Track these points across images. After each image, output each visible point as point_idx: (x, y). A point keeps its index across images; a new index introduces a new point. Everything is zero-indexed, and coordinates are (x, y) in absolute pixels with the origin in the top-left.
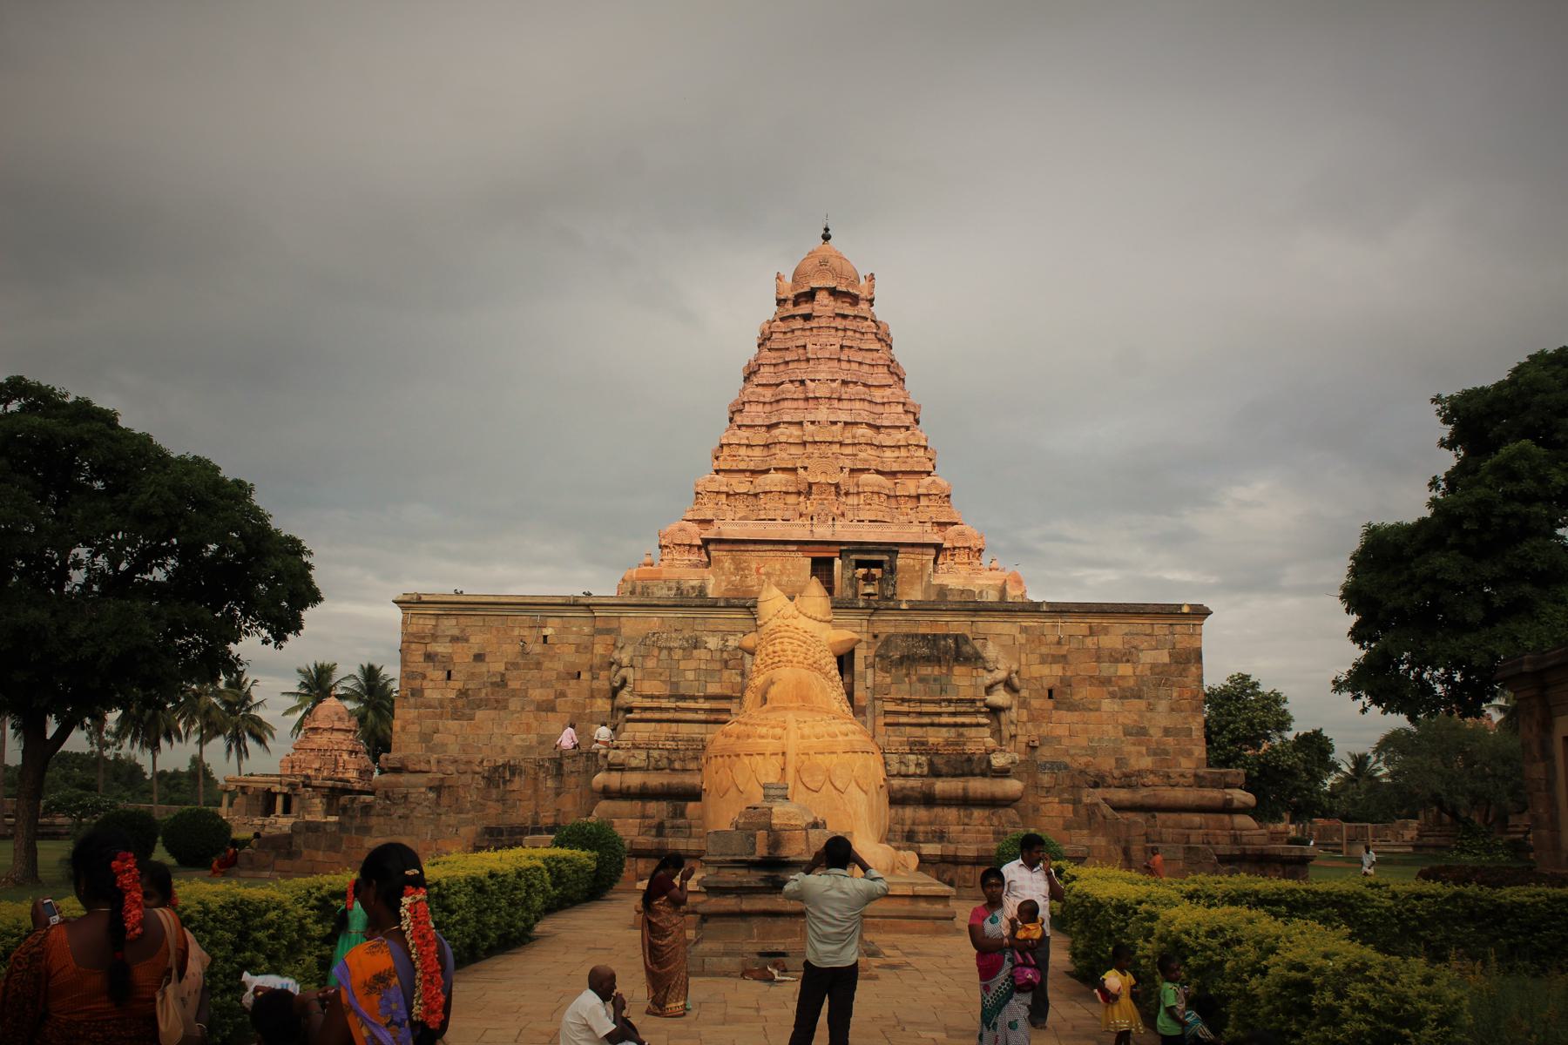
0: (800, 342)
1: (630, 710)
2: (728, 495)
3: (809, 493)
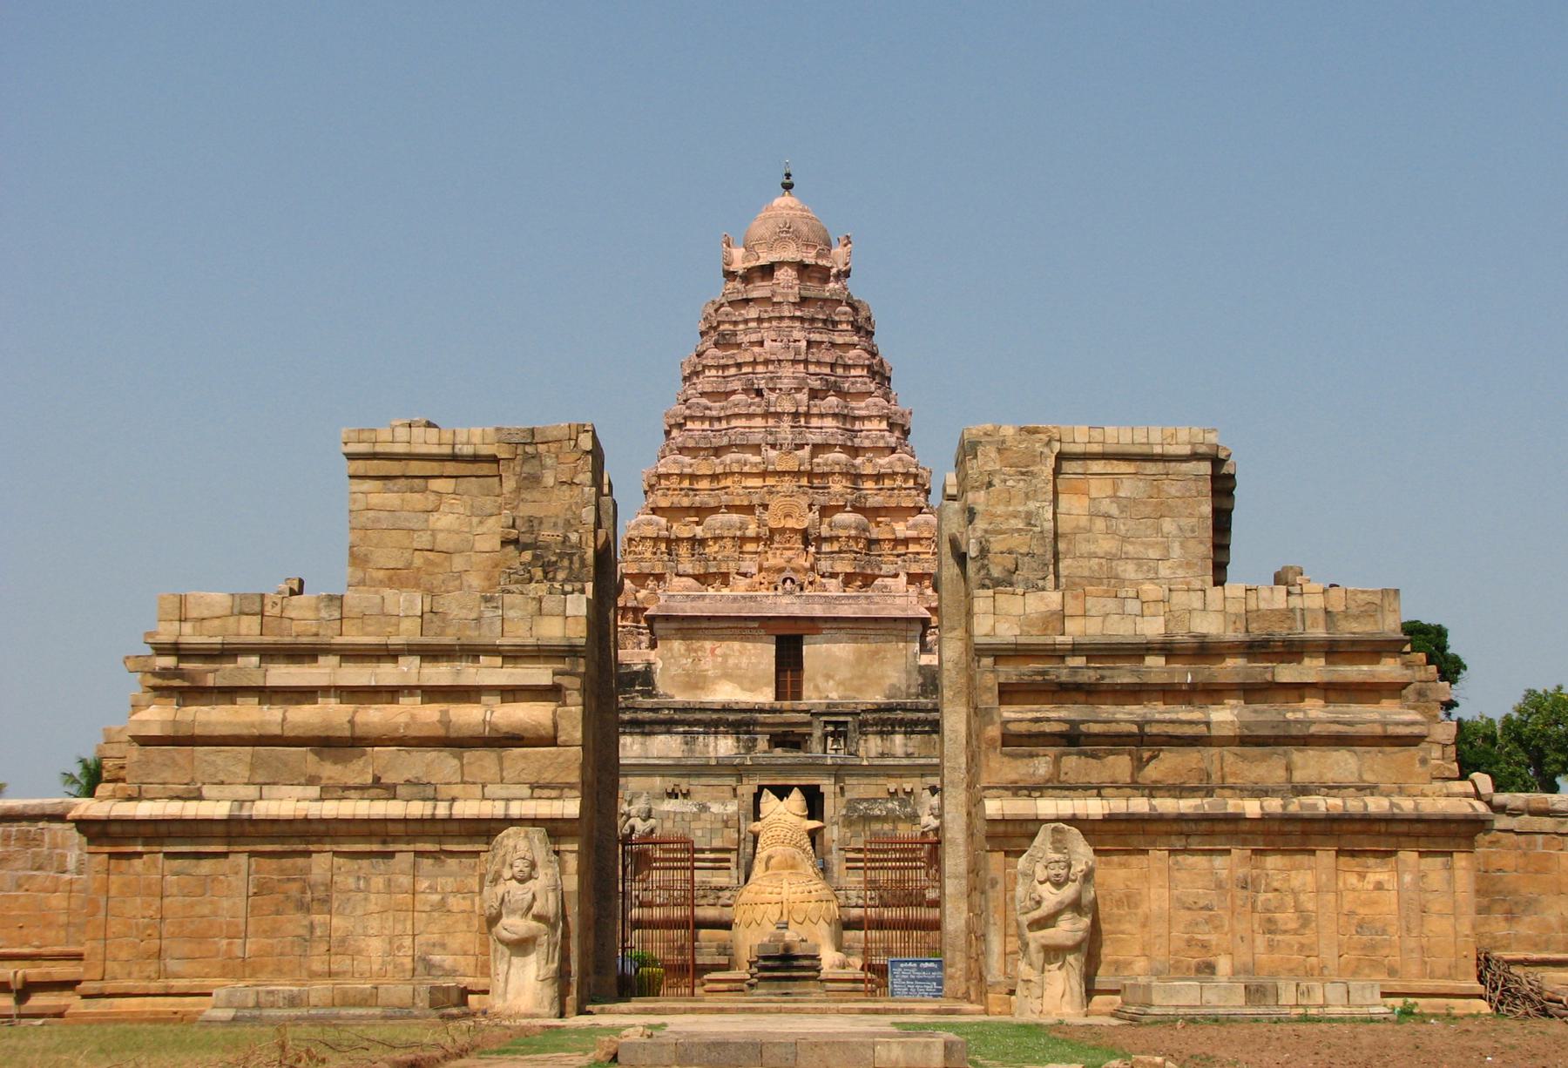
0: (754, 337)
1: (656, 860)
2: (668, 541)
3: (771, 539)
